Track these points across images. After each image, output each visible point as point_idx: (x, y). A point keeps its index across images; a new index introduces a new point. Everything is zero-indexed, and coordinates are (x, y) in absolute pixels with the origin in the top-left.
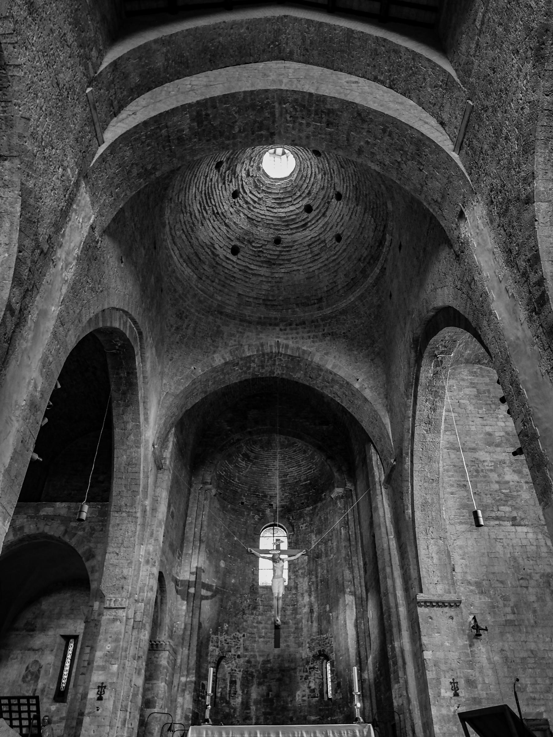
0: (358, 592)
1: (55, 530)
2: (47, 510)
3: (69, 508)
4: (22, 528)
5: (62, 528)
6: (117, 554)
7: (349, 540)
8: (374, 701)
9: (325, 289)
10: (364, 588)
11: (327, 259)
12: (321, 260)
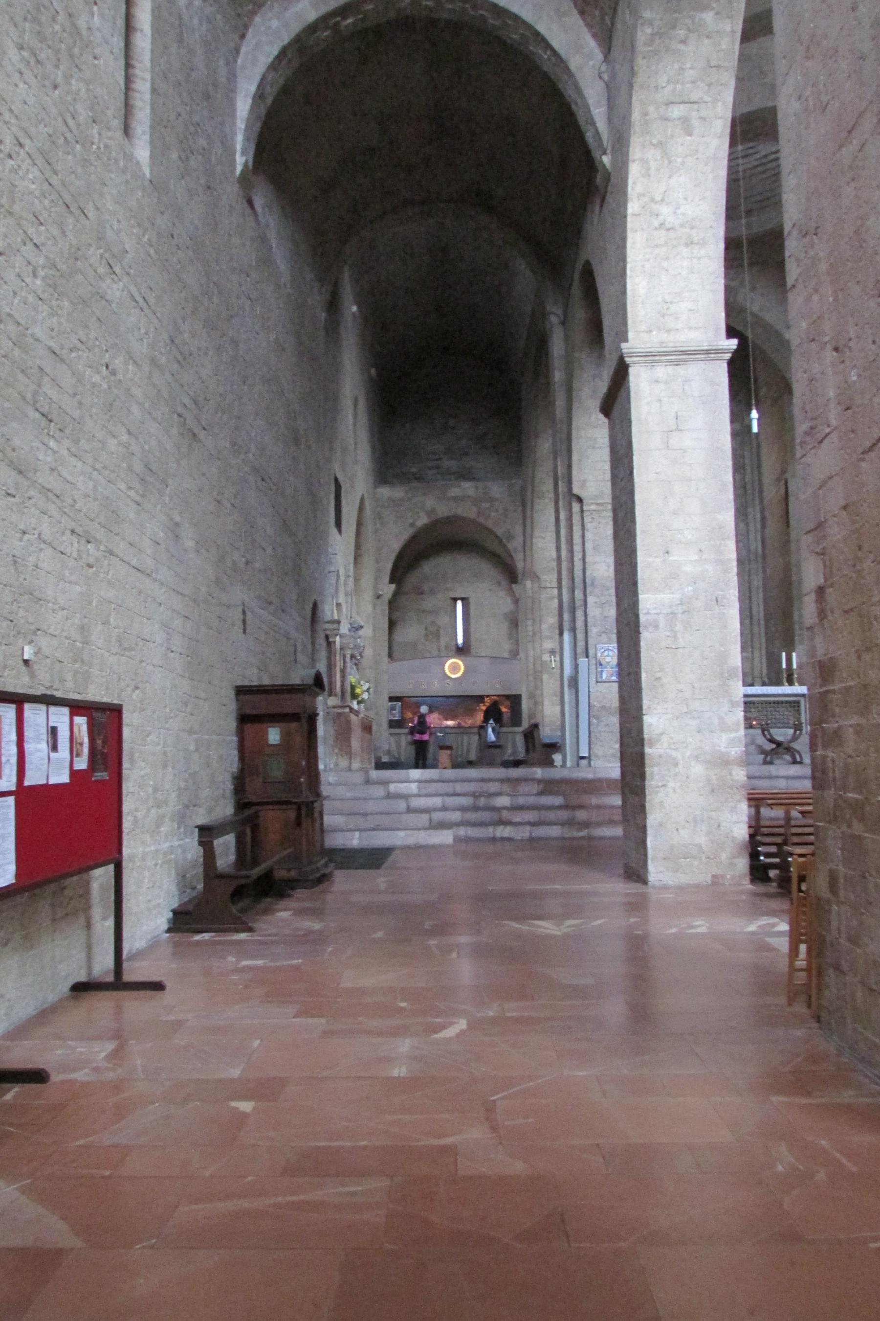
0: (753, 547)
1: (468, 511)
2: (454, 492)
3: (477, 488)
4: (433, 511)
5: (475, 509)
6: (544, 538)
7: (745, 488)
8: (764, 652)
9: (758, 198)
10: (760, 543)
11: (765, 156)
12: (758, 156)
